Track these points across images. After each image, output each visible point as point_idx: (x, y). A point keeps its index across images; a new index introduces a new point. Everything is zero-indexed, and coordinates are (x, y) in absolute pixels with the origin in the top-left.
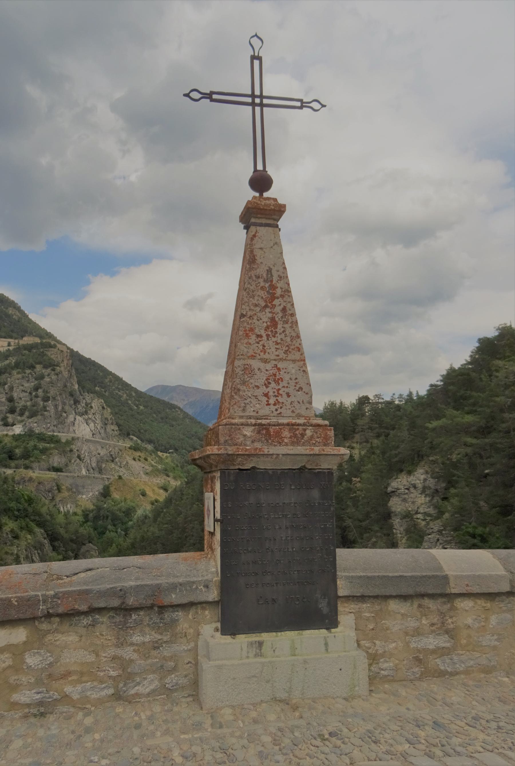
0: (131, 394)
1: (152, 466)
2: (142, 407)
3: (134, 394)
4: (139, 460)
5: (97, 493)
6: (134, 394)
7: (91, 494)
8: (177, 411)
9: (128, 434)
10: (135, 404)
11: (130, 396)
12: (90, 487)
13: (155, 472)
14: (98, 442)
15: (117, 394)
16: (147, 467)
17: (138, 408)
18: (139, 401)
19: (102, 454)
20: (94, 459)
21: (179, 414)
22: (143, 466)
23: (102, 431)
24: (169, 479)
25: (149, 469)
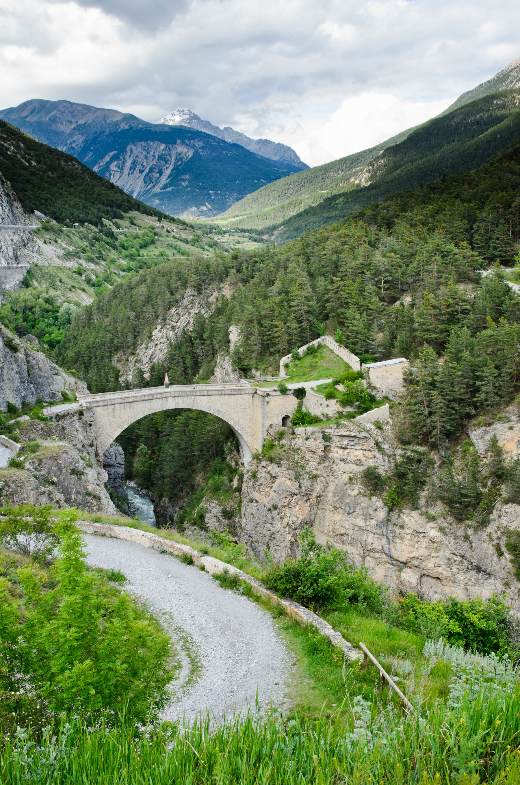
0: (20, 146)
1: (64, 249)
2: (34, 164)
3: (22, 146)
4: (50, 243)
5: (18, 282)
6: (22, 146)
7: (13, 283)
8: (74, 165)
9: (32, 212)
10: (25, 159)
11: (17, 147)
12: (12, 277)
13: (69, 255)
14: (9, 228)
15: (3, 145)
16: (58, 251)
17: (31, 164)
18: (29, 154)
19: (14, 240)
20: (10, 249)
21: (77, 169)
22: (55, 249)
23: (10, 214)
24: (81, 261)
25: (62, 252)
